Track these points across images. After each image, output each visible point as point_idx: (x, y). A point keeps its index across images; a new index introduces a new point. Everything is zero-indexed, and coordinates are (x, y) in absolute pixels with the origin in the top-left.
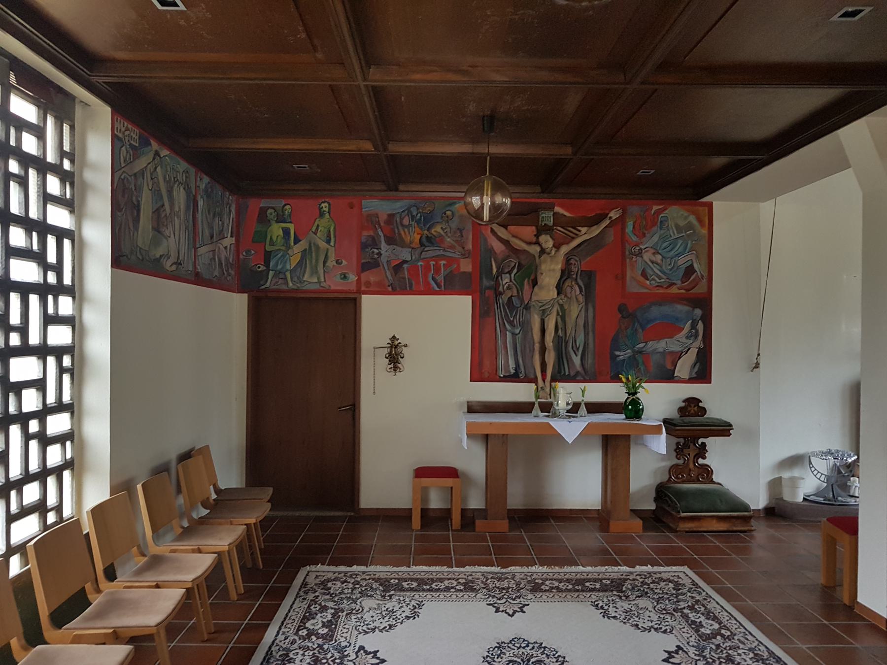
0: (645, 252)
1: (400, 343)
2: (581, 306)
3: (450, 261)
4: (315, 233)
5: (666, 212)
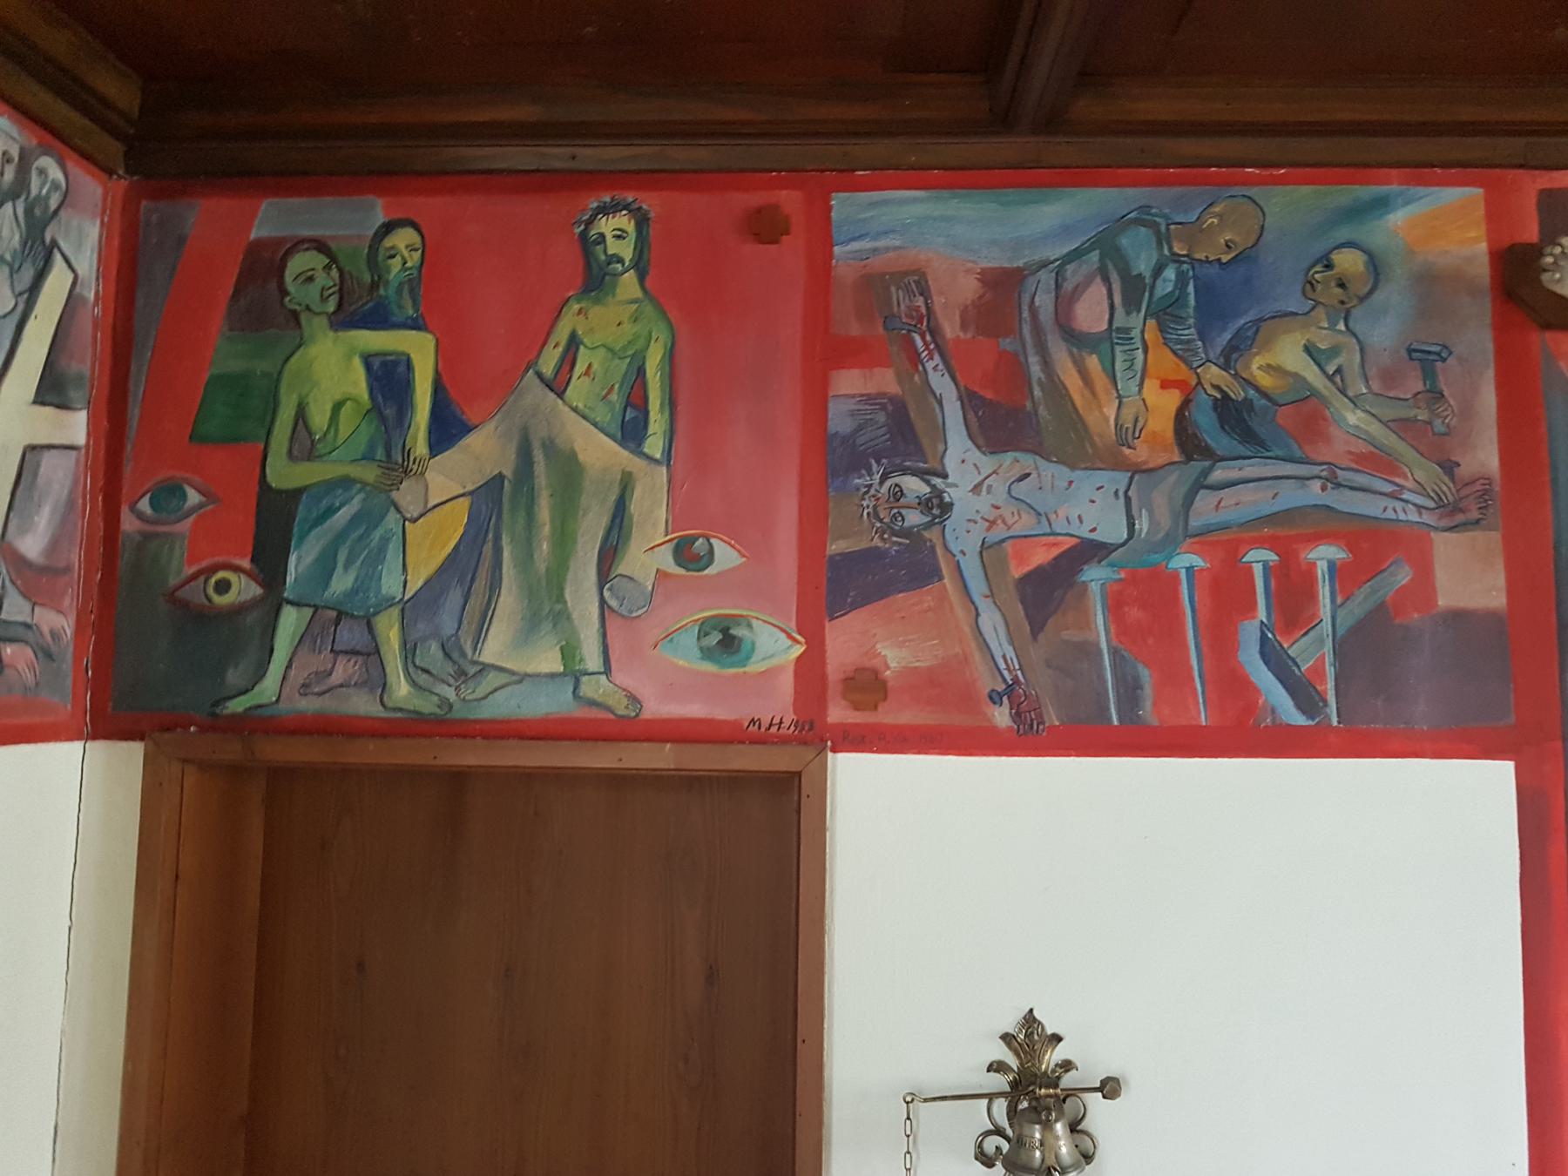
1: (1067, 1066)
4: (557, 385)
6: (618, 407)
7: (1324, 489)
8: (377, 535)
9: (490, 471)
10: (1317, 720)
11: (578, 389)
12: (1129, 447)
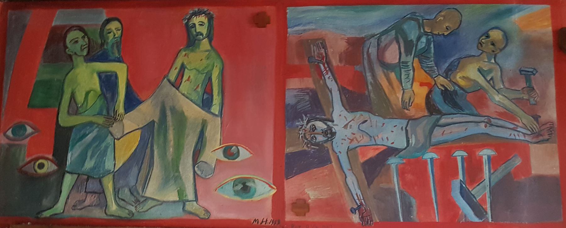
4: (176, 85)
6: (201, 93)
7: (486, 126)
8: (103, 145)
9: (149, 120)
10: (483, 220)
11: (185, 86)
12: (407, 110)
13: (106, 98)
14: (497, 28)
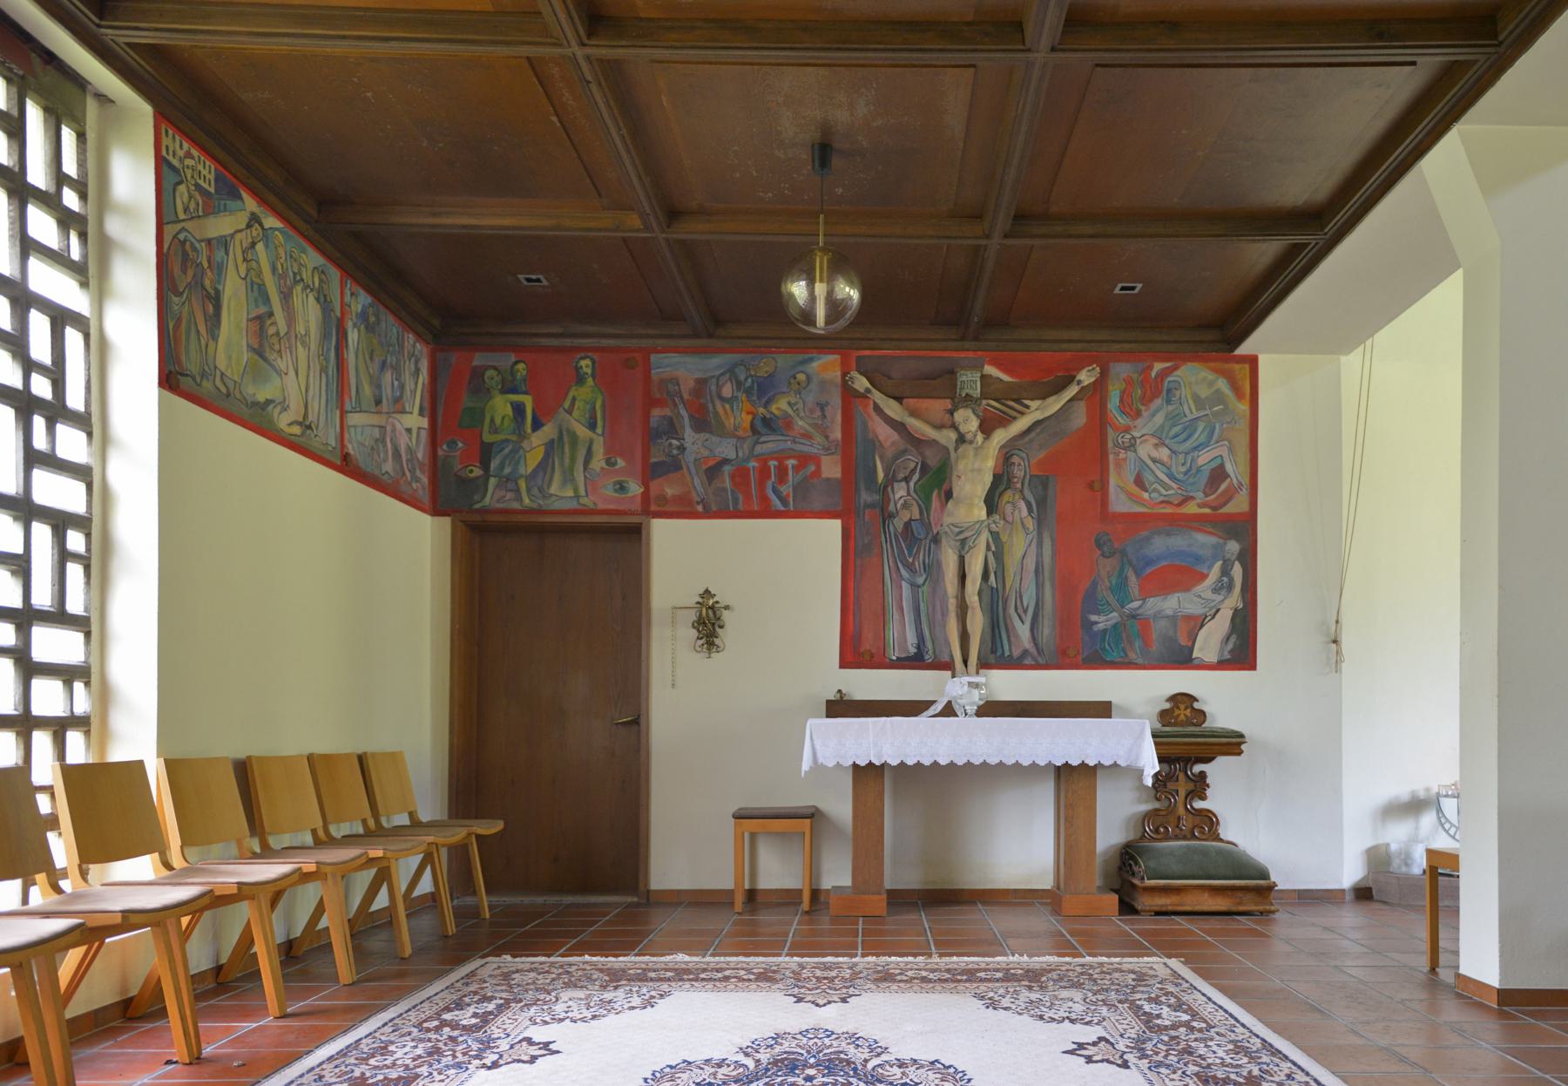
0: (1141, 443)
1: (717, 602)
2: (1030, 537)
3: (804, 460)
4: (570, 412)
5: (1178, 373)
8: (517, 456)
11: (576, 413)
13: (517, 422)
14: (802, 372)
